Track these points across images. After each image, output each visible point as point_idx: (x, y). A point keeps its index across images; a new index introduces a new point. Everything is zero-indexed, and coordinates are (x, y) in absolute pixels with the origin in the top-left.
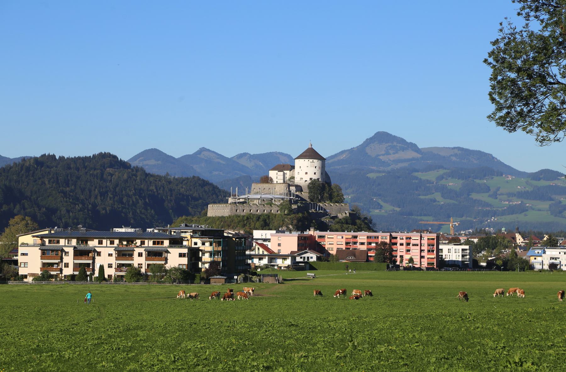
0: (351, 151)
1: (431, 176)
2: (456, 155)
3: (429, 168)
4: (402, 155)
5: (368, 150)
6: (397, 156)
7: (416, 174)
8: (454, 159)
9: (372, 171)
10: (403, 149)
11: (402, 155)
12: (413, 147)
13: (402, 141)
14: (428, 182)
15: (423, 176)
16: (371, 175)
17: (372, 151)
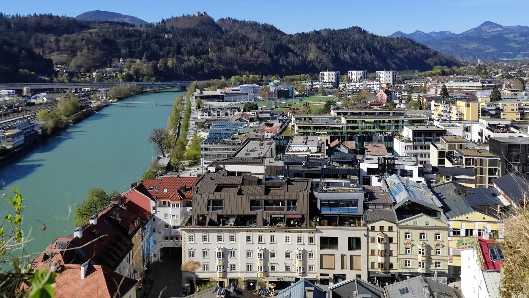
0: (475, 29)
1: (511, 36)
2: (518, 28)
3: (509, 33)
4: (495, 29)
5: (482, 28)
6: (493, 30)
7: (504, 36)
8: (517, 30)
9: (485, 35)
10: (496, 27)
11: (495, 29)
12: (500, 26)
13: (496, 24)
14: (509, 38)
15: (507, 36)
16: (485, 37)
17: (483, 29)
